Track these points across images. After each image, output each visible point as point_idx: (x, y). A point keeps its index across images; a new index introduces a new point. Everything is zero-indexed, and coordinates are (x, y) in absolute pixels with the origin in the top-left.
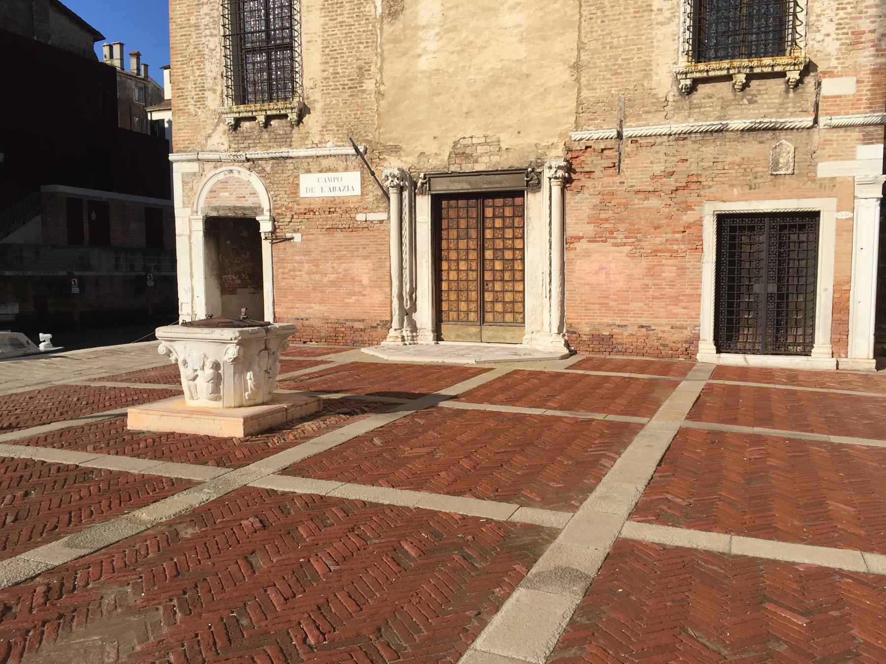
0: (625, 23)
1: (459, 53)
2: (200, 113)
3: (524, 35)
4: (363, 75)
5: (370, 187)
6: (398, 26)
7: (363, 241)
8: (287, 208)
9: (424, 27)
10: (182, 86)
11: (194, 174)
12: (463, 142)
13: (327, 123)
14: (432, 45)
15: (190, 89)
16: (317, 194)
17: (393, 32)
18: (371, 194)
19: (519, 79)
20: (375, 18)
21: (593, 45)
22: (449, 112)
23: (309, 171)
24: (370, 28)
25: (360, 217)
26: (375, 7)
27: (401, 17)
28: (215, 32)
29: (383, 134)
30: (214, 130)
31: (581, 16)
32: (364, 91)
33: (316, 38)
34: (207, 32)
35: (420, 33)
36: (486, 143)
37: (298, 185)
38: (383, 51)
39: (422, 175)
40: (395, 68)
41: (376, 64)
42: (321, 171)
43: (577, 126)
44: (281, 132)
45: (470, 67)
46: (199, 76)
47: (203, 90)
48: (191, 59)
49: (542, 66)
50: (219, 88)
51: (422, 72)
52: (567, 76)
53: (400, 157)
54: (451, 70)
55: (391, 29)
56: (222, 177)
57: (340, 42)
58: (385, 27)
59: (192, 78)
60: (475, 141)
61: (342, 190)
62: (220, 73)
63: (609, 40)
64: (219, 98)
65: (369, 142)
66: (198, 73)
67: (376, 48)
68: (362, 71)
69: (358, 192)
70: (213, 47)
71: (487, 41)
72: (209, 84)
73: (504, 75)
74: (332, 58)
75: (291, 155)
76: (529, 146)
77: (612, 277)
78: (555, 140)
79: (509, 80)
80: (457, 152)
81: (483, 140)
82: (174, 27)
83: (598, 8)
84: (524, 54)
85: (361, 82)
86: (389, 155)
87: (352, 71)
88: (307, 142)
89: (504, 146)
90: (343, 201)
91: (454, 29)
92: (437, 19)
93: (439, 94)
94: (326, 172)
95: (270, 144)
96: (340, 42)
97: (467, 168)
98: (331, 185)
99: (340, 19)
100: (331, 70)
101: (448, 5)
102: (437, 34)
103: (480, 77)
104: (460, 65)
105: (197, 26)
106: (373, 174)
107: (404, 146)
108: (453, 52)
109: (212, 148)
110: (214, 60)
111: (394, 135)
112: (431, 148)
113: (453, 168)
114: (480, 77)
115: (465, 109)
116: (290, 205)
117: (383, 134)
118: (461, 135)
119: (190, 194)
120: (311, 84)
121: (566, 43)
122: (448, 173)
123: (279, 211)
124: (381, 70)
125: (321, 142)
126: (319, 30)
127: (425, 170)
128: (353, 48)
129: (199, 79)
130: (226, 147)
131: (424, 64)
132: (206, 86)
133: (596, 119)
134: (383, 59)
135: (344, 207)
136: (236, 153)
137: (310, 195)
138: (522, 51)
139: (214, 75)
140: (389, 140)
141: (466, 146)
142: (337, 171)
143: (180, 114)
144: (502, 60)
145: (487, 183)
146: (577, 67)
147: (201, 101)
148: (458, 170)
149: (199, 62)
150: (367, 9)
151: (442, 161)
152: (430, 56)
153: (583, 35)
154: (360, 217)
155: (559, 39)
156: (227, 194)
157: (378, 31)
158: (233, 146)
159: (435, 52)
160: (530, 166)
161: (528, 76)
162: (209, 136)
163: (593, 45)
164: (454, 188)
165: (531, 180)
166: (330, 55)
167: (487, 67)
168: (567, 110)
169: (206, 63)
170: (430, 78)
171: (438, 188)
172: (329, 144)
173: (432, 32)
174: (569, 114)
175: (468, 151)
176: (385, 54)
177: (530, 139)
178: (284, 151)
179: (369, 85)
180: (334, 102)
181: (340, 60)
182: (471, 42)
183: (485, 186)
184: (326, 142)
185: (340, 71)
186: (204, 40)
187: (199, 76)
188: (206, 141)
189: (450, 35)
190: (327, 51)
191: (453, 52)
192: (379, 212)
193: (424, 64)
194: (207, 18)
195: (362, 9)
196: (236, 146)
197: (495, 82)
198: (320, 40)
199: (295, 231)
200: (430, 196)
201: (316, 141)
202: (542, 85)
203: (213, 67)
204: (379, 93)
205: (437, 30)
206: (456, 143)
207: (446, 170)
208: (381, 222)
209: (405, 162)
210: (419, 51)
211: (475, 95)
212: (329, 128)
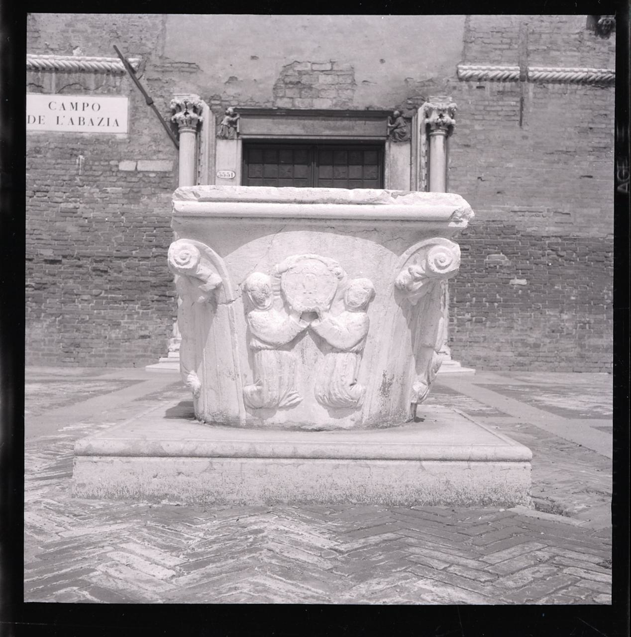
5: (146, 121)
18: (146, 132)
39: (230, 109)
61: (96, 122)
65: (146, 55)
80: (287, 80)
81: (328, 67)
97: (301, 104)
122: (271, 110)
127: (235, 103)
145: (331, 128)
148: (289, 106)
160: (397, 108)
164: (279, 132)
165: (396, 128)
171: (253, 131)
175: (305, 80)
183: (328, 132)
192: (158, 159)
200: (240, 142)
207: (269, 105)
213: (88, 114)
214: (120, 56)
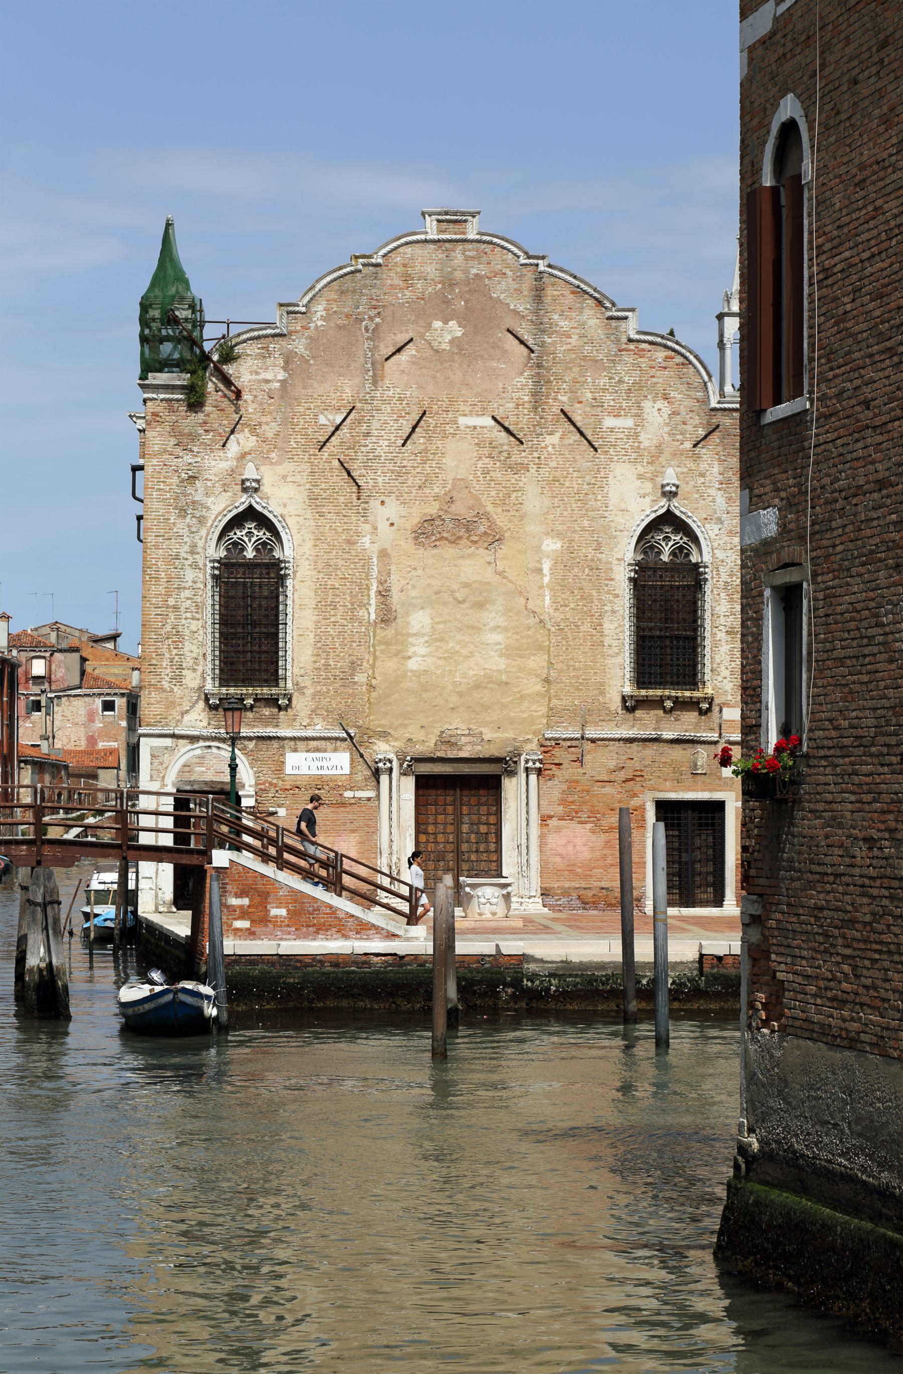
0: (584, 653)
1: (445, 658)
2: (175, 690)
3: (504, 651)
4: (354, 669)
6: (390, 632)
7: (350, 816)
8: (271, 784)
9: (414, 635)
10: (154, 662)
11: (166, 748)
12: (450, 733)
13: (317, 708)
14: (422, 650)
15: (164, 666)
16: (304, 772)
17: (385, 636)
19: (499, 685)
20: (369, 622)
21: (558, 666)
22: (435, 706)
23: (295, 750)
24: (363, 630)
25: (348, 794)
26: (369, 613)
27: (394, 624)
28: (198, 616)
29: (373, 721)
30: (192, 707)
31: (550, 642)
32: (355, 683)
33: (308, 633)
34: (189, 615)
35: (410, 640)
36: (469, 735)
37: (283, 763)
38: (375, 651)
39: (408, 758)
40: (387, 665)
41: (368, 661)
42: (308, 751)
43: (549, 726)
44: (267, 713)
45: (456, 671)
46: (177, 655)
47: (181, 668)
48: (167, 638)
49: (518, 678)
50: (200, 669)
51: (412, 671)
52: (539, 688)
53: (387, 742)
54: (438, 672)
55: (383, 634)
56: (198, 752)
57: (333, 639)
58: (378, 631)
59: (167, 655)
60: (459, 732)
62: (201, 654)
63: (572, 663)
64: (199, 678)
65: (358, 727)
66: (175, 652)
67: (369, 647)
68: (354, 666)
69: (347, 770)
70: (195, 630)
71: (471, 652)
72: (188, 662)
73: (486, 680)
74: (323, 652)
75: (278, 735)
76: (508, 739)
77: (578, 848)
78: (530, 737)
79: (490, 686)
81: (467, 732)
82: (148, 605)
83: (563, 638)
84: (504, 667)
85: (352, 675)
86: (378, 739)
87: (344, 664)
88: (294, 724)
89: (486, 737)
90: (332, 779)
91: (442, 640)
92: (427, 630)
93: (426, 691)
94: (314, 752)
95: (256, 724)
96: (333, 639)
98: (319, 764)
99: (333, 619)
100: (323, 661)
101: (436, 620)
102: (426, 642)
103: (465, 680)
104: (447, 669)
105: (176, 608)
106: (362, 756)
107: (392, 732)
108: (440, 658)
109: (189, 724)
110: (195, 642)
111: (383, 722)
112: (418, 736)
113: (439, 754)
114: (465, 680)
115: (452, 705)
116: (275, 781)
117: (373, 721)
118: (446, 726)
119: (160, 767)
120: (302, 672)
121: (537, 662)
123: (262, 787)
124: (373, 666)
125: (309, 725)
126: (311, 626)
127: (411, 754)
128: (346, 645)
129: (176, 657)
130: (205, 723)
131: (412, 664)
132: (184, 665)
133: (563, 722)
134: (375, 660)
135: (331, 784)
136: (216, 731)
137: (296, 772)
138: (502, 663)
139: (194, 655)
140: (379, 727)
141: (451, 736)
142: (325, 751)
143: (151, 689)
144: (484, 669)
146: (547, 681)
147: (178, 679)
148: (444, 756)
149: (176, 642)
150: (360, 614)
151: (429, 747)
152: (419, 659)
153: (551, 658)
154: (348, 794)
155: (532, 658)
156: (204, 769)
157: (372, 634)
158: (213, 722)
159: (424, 656)
161: (506, 683)
162: (187, 712)
163: (558, 666)
166: (322, 648)
167: (471, 673)
168: (540, 713)
169: (187, 643)
170: (419, 677)
172: (318, 727)
173: (422, 640)
174: (543, 716)
175: (453, 740)
176: (377, 653)
177: (510, 735)
178: (270, 731)
179: (361, 678)
180: (325, 690)
181: (332, 654)
182: (458, 652)
184: (315, 725)
185: (332, 663)
186: (183, 621)
187: (177, 655)
188: (182, 717)
189: (438, 644)
190: (319, 645)
191: (440, 658)
193: (412, 664)
194: (189, 602)
195: (355, 613)
196: (216, 723)
197: (477, 686)
198: (312, 636)
199: (279, 806)
201: (304, 724)
202: (519, 692)
203: (194, 648)
204: (371, 686)
205: (426, 638)
206: (442, 732)
207: (432, 755)
208: (369, 799)
209: (393, 746)
210: (410, 654)
211: (460, 694)
212: (318, 712)
213: (325, 764)
214: (344, 729)
